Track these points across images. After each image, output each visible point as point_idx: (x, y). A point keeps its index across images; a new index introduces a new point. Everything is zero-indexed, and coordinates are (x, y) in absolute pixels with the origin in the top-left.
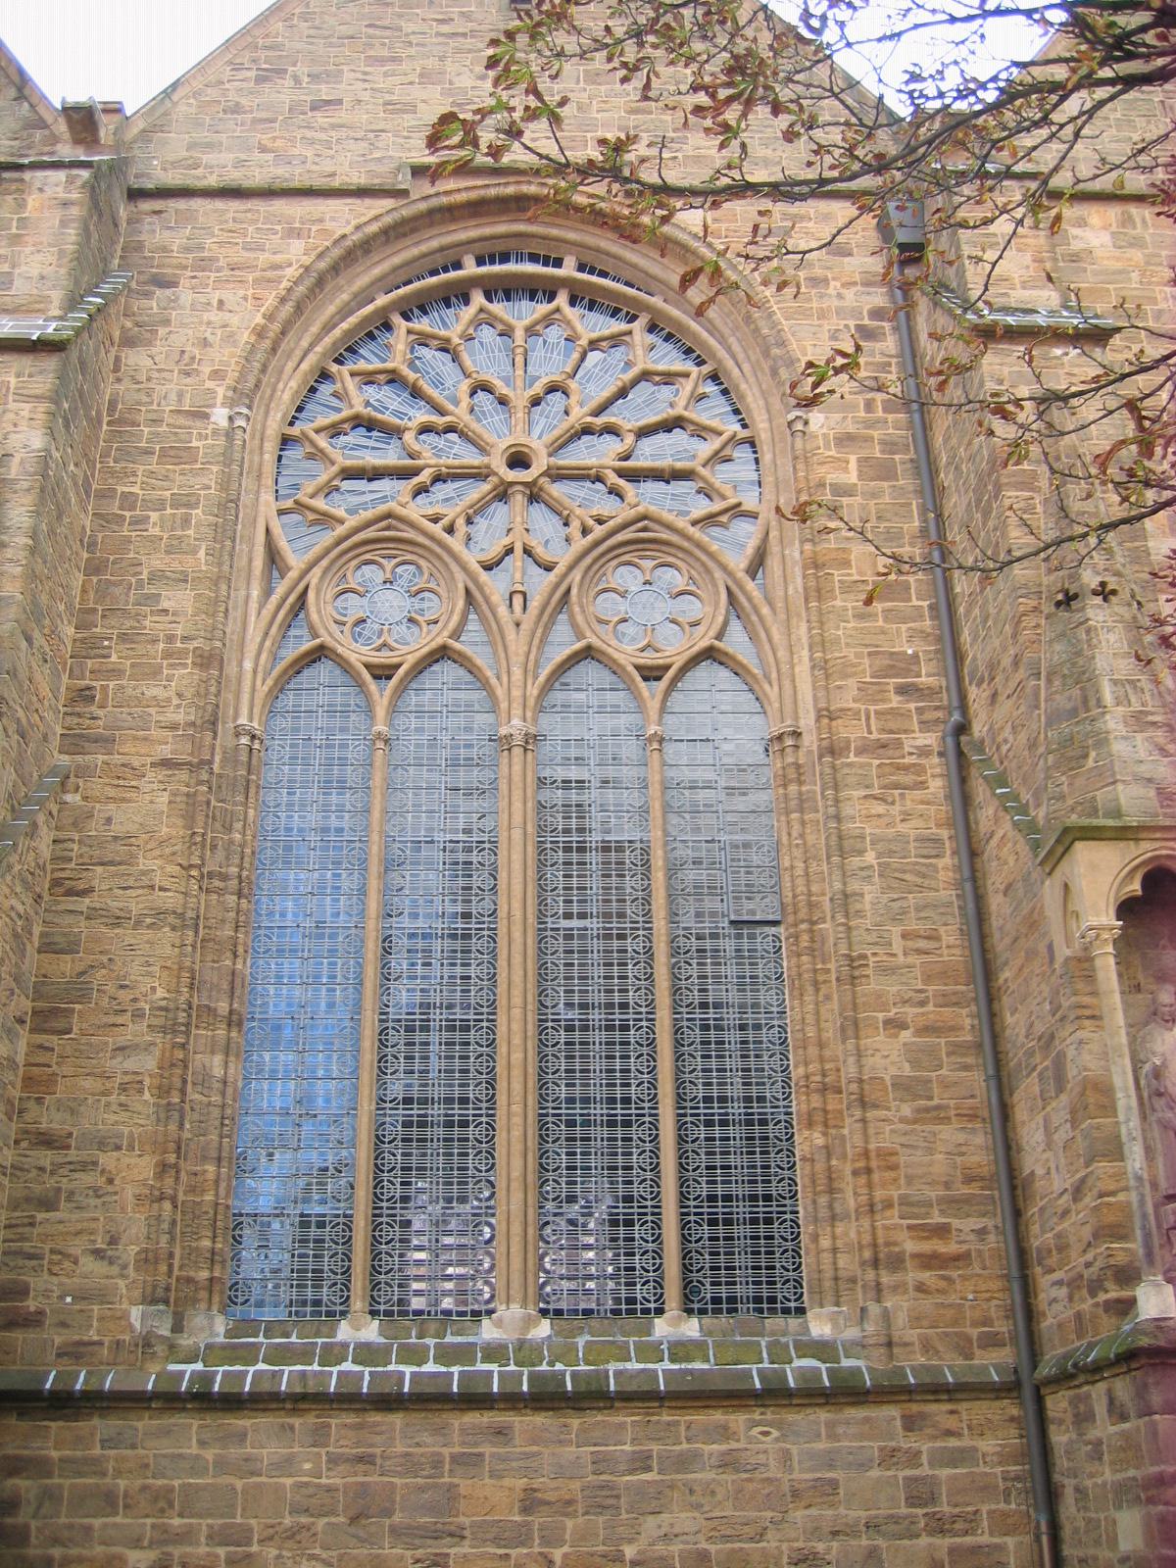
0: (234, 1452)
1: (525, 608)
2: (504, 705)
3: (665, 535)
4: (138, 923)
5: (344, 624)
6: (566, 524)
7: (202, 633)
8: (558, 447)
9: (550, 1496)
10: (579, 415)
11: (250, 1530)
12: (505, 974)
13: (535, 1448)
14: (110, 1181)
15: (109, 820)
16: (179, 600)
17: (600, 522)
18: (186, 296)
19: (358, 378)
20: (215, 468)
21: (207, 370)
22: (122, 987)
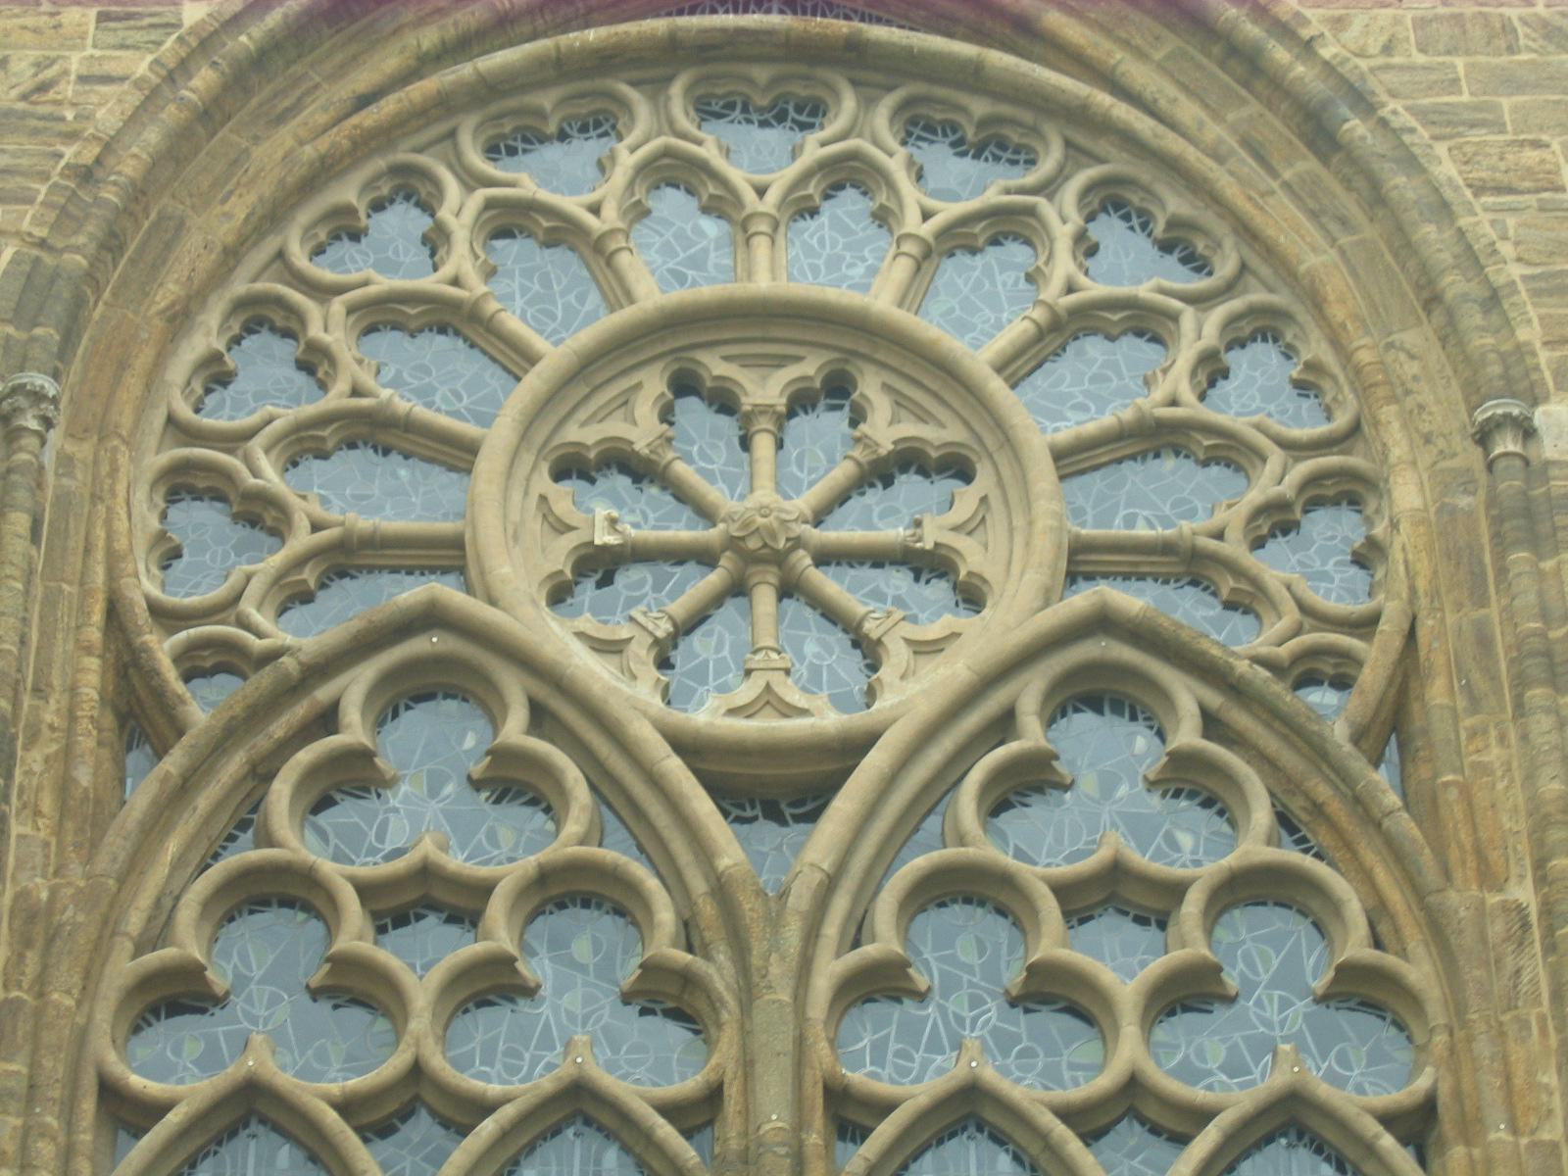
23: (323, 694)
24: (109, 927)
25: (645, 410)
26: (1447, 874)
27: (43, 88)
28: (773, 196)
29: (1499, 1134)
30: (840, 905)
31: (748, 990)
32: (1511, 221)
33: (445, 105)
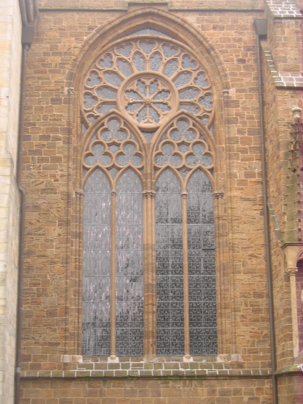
23: (102, 122)
24: (83, 149)
25: (135, 85)
26: (216, 143)
27: (70, 49)
28: (149, 57)
30: (156, 146)
31: (146, 156)
32: (228, 65)
33: (113, 46)
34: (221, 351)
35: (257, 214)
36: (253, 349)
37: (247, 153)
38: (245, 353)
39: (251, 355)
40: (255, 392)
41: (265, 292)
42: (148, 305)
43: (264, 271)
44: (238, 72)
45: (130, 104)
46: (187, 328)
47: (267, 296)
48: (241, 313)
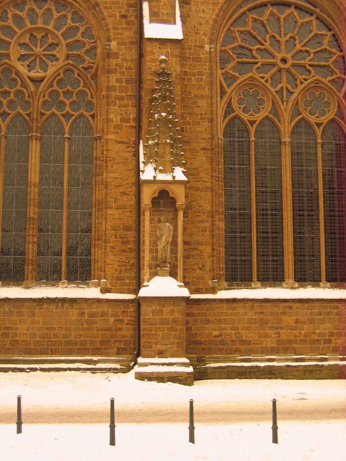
0: (234, 311)
1: (287, 105)
2: (283, 133)
3: (322, 85)
4: (202, 191)
5: (240, 108)
6: (296, 80)
7: (209, 113)
8: (293, 57)
9: (301, 320)
10: (298, 47)
11: (239, 328)
12: (285, 203)
13: (298, 311)
14: (201, 252)
15: (192, 164)
16: (203, 103)
17: (306, 80)
18: (194, 8)
19: (239, 32)
20: (207, 64)
21: (202, 33)
22: (200, 206)
25: (27, 39)
28: (41, 13)
29: (99, 118)
30: (42, 94)
31: (33, 103)
34: (93, 277)
35: (129, 155)
36: (121, 277)
37: (124, 101)
38: (113, 280)
39: (118, 281)
40: (120, 315)
41: (134, 225)
42: (29, 236)
43: (134, 207)
44: (120, 27)
45: (22, 56)
46: (64, 257)
47: (135, 230)
48: (111, 244)
